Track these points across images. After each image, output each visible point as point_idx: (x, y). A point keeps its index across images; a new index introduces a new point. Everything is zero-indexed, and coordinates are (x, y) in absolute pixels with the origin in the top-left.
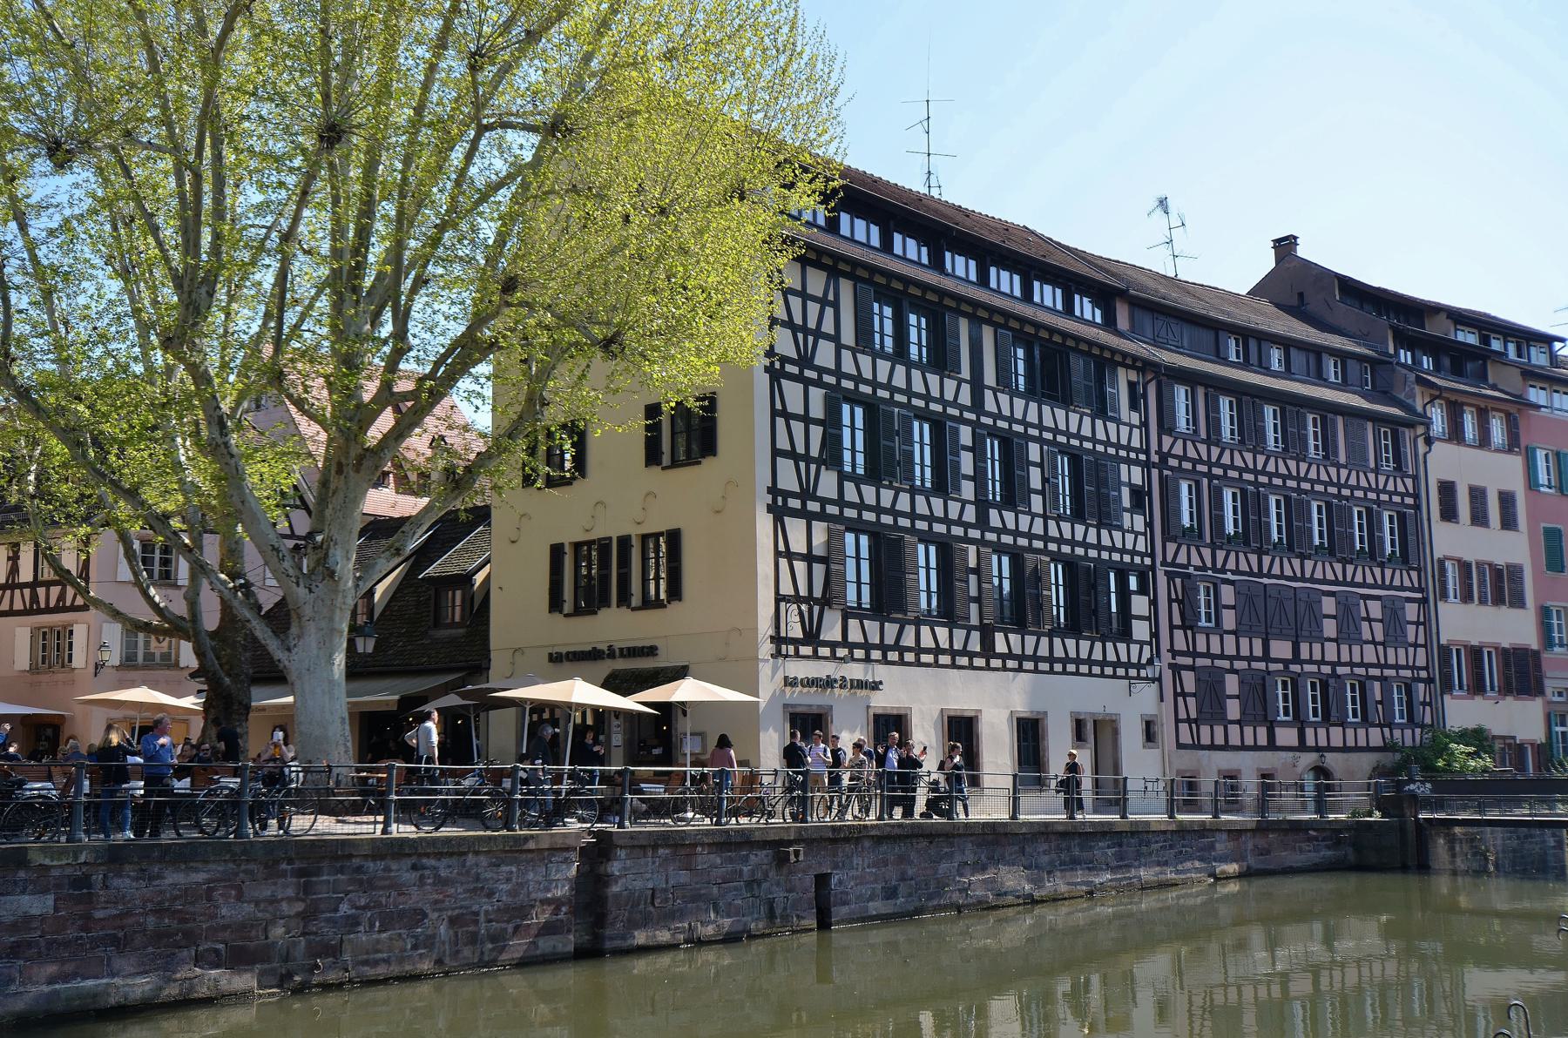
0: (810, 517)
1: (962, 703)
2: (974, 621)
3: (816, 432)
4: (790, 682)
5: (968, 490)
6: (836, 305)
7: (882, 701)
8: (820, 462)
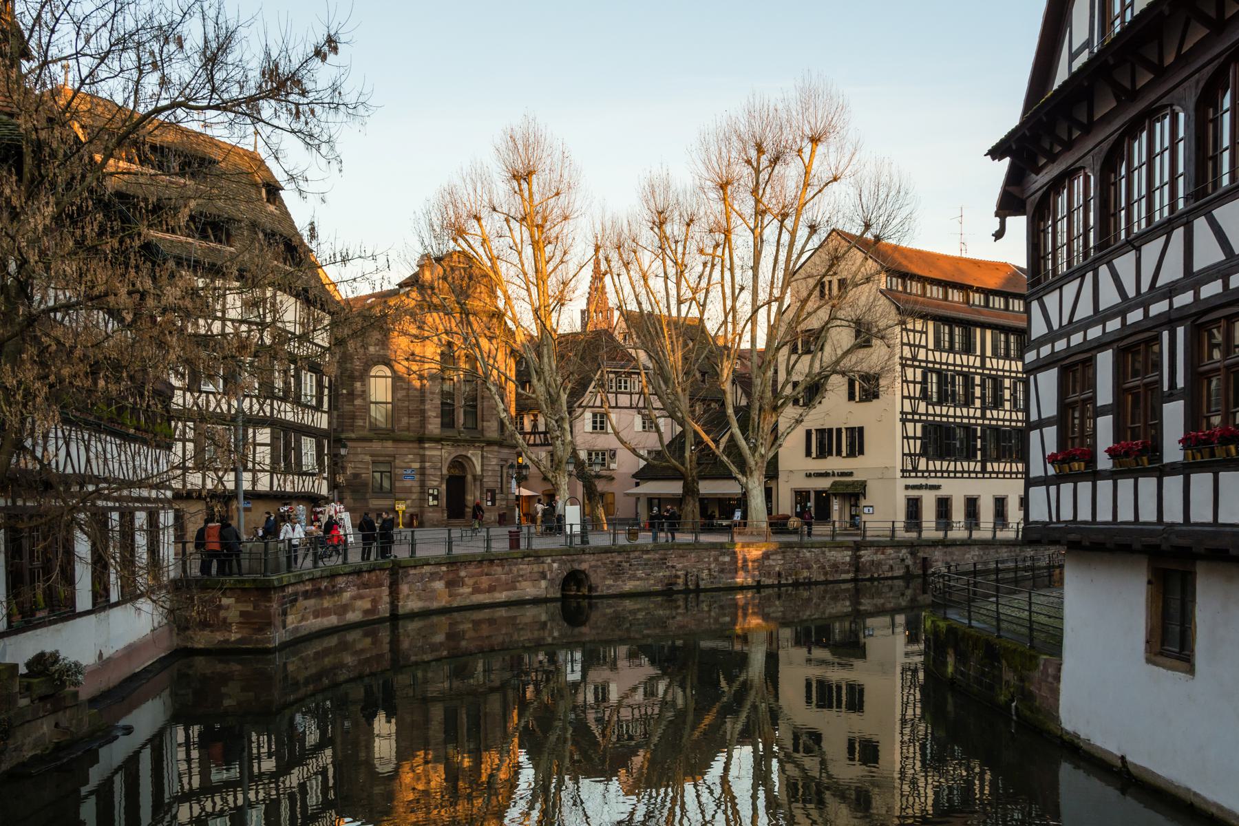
0: (915, 421)
1: (972, 493)
2: (979, 458)
3: (918, 387)
4: (907, 487)
5: (978, 403)
6: (926, 333)
7: (942, 493)
8: (919, 399)
